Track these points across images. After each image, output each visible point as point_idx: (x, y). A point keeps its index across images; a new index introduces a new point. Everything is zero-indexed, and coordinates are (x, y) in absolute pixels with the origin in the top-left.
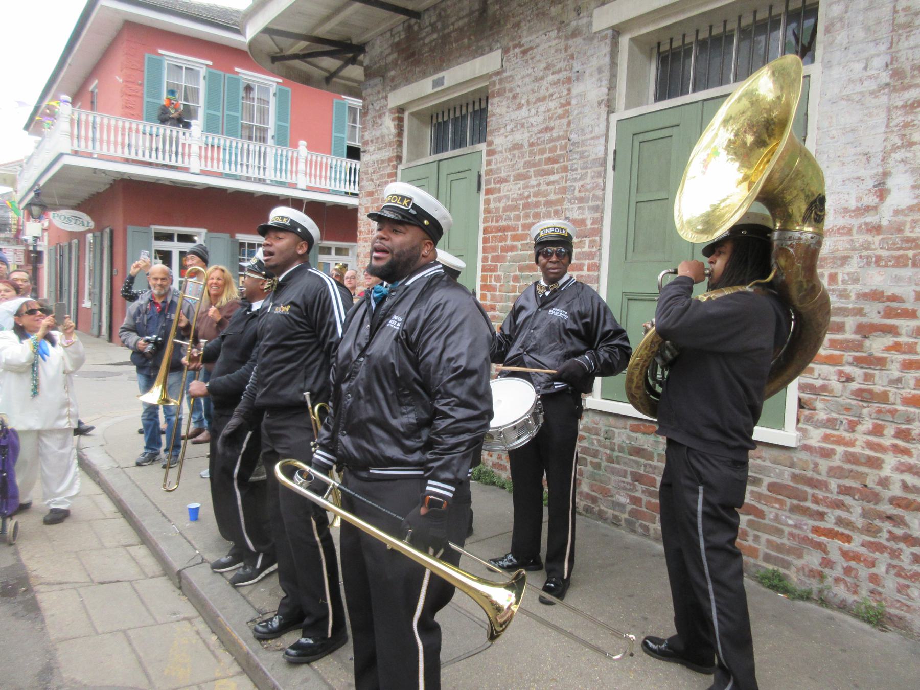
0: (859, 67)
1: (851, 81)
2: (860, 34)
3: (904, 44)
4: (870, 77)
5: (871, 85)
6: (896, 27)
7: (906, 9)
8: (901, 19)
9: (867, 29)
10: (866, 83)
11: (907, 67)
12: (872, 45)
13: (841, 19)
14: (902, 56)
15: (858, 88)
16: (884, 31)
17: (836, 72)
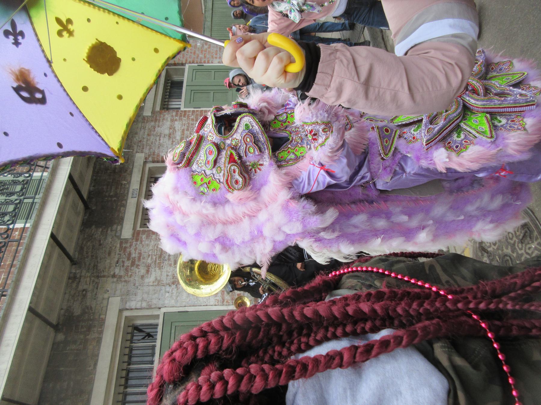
0: (167, 294)
1: (171, 297)
2: (156, 295)
3: (164, 282)
4: (172, 291)
5: (175, 291)
6: (158, 285)
7: (153, 282)
8: (156, 283)
9: (155, 293)
10: (174, 292)
11: (172, 280)
12: (161, 291)
13: (148, 302)
14: (168, 282)
15: (175, 294)
16: (158, 288)
17: (166, 302)
